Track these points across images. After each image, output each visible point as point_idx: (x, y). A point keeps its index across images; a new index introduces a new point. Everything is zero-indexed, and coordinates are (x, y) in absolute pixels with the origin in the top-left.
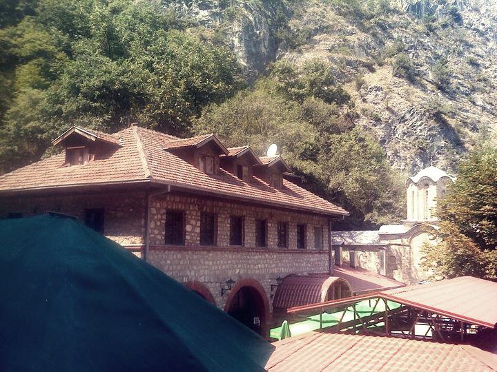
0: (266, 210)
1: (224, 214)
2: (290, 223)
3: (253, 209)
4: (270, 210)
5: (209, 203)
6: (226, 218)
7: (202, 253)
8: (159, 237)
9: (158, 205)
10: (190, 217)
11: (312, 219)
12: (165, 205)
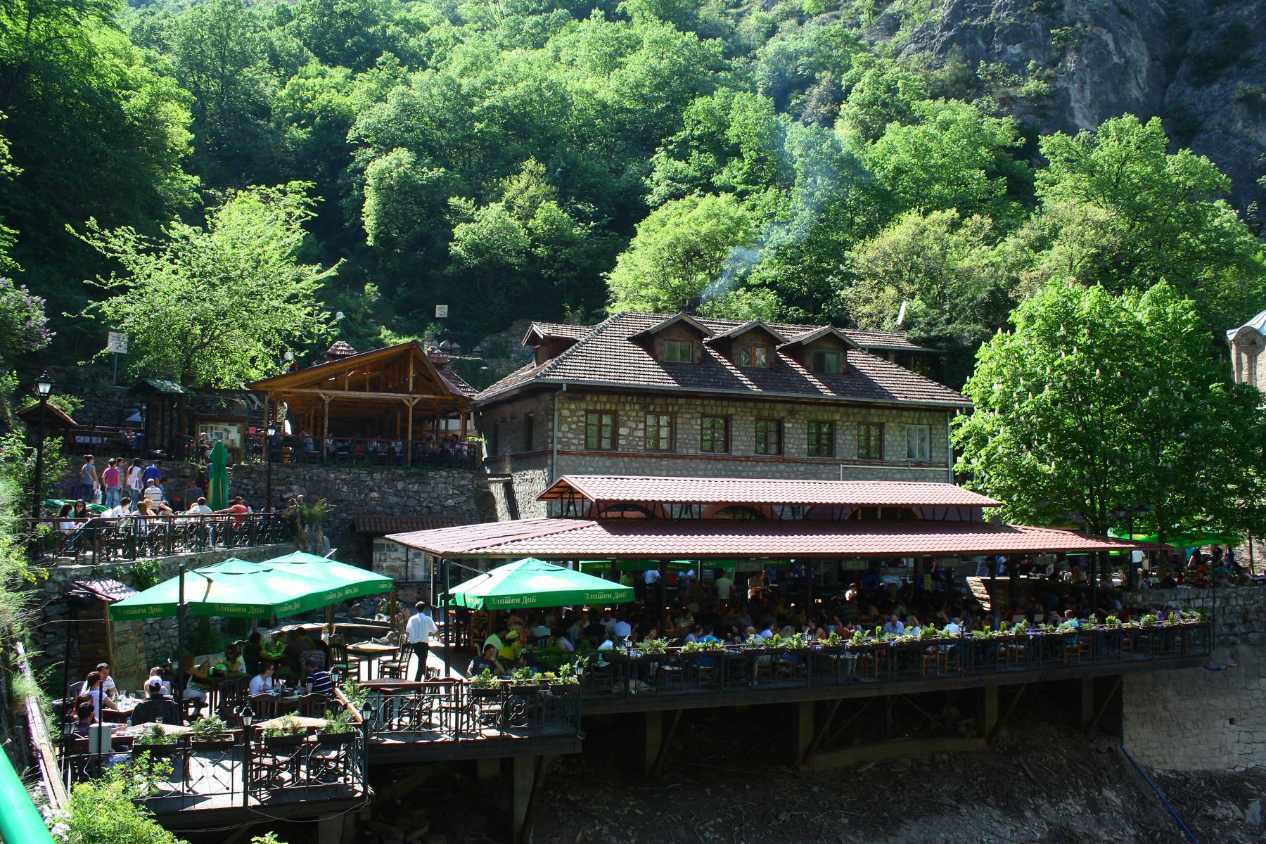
0: (779, 406)
1: (689, 413)
2: (839, 423)
3: (750, 404)
4: (789, 406)
5: (659, 401)
6: (692, 418)
7: (648, 460)
8: (575, 441)
9: (573, 406)
10: (625, 418)
11: (900, 417)
12: (583, 406)
